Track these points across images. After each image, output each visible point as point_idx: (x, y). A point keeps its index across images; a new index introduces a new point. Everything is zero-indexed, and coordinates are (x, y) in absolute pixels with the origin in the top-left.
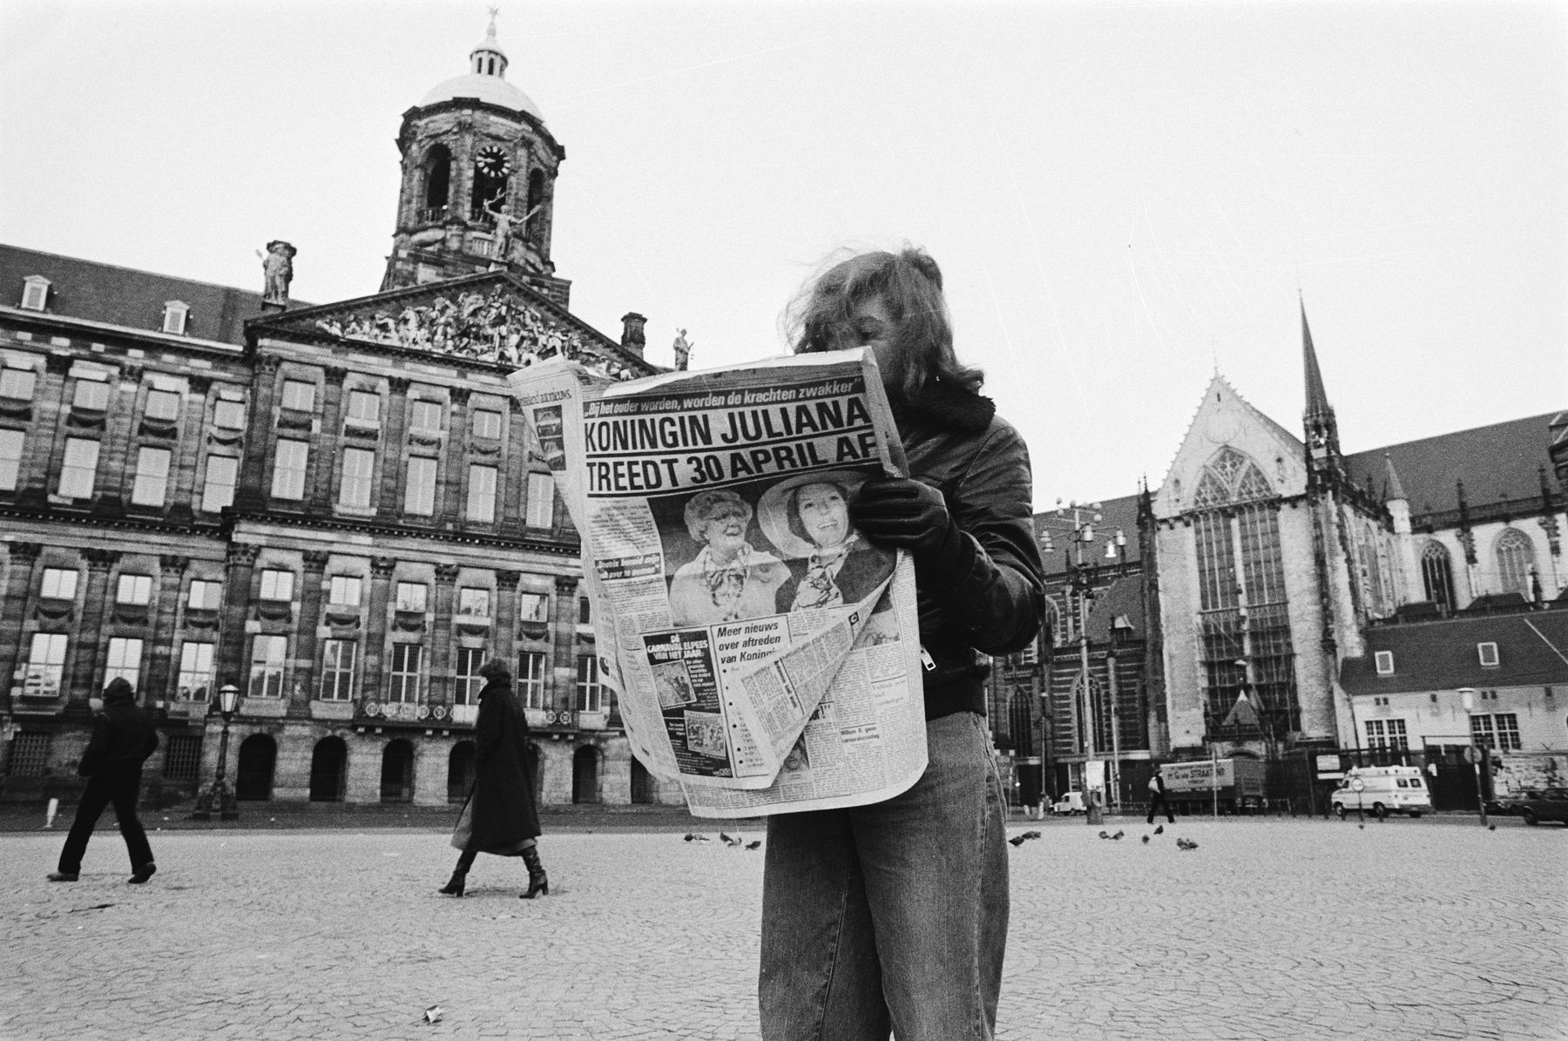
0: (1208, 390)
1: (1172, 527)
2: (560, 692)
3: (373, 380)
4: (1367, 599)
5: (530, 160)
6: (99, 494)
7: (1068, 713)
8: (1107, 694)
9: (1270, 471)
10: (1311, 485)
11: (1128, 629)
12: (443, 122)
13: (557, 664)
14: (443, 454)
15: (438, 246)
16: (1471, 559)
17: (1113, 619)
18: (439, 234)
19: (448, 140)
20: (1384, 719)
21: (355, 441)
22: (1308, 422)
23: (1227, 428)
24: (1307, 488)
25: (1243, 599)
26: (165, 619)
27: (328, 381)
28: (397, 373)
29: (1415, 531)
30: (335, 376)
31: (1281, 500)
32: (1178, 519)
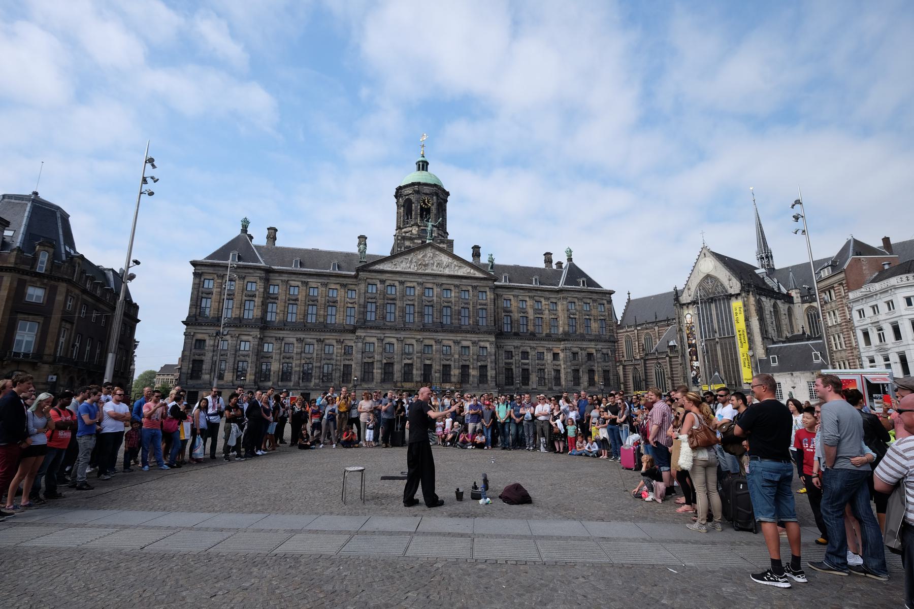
0: (701, 252)
1: (688, 307)
3: (393, 282)
4: (772, 332)
5: (437, 199)
7: (652, 378)
9: (726, 283)
10: (743, 289)
11: (675, 346)
14: (416, 304)
17: (668, 342)
18: (410, 229)
19: (412, 197)
21: (389, 302)
22: (759, 256)
23: (709, 266)
24: (741, 291)
25: (717, 335)
26: (339, 358)
28: (400, 279)
31: (731, 295)
32: (689, 304)
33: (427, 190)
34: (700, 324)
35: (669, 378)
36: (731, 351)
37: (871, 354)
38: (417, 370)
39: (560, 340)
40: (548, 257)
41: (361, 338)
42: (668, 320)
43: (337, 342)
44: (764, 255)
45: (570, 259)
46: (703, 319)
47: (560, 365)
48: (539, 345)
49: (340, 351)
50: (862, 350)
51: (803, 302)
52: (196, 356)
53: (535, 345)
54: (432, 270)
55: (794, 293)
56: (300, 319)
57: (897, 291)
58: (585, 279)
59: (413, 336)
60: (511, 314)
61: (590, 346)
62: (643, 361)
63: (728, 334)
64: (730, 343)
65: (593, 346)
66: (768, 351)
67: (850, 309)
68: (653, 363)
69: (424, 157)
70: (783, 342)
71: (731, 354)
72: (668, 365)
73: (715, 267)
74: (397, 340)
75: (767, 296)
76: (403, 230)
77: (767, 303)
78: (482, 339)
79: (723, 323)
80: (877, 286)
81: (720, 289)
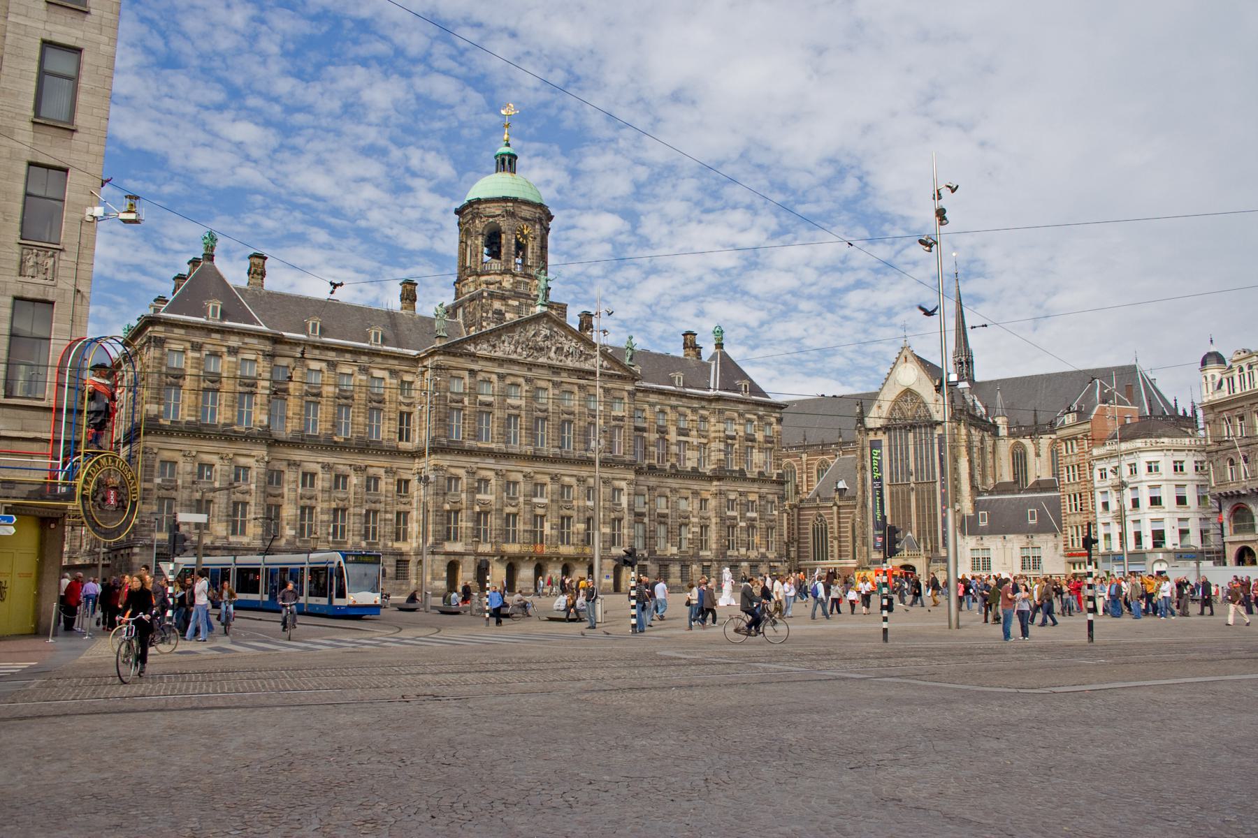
2: (581, 537)
3: (489, 375)
6: (355, 435)
8: (832, 528)
12: (495, 209)
13: (578, 522)
14: (523, 413)
15: (497, 285)
16: (1038, 455)
18: (498, 278)
20: (980, 547)
23: (909, 375)
25: (913, 479)
27: (470, 377)
29: (1011, 435)
30: (473, 373)
32: (879, 429)
33: (526, 212)
34: (891, 460)
35: (835, 538)
36: (929, 502)
37: (1107, 521)
38: (524, 523)
39: (710, 479)
40: (690, 340)
41: (442, 470)
42: (823, 445)
43: (386, 472)
44: (963, 359)
45: (719, 346)
46: (896, 454)
47: (709, 518)
48: (682, 486)
49: (390, 488)
50: (1098, 516)
51: (1011, 435)
52: (164, 491)
53: (678, 486)
54: (549, 358)
55: (1000, 421)
56: (326, 429)
57: (1141, 455)
58: (747, 383)
59: (519, 468)
60: (645, 434)
61: (752, 490)
62: (796, 510)
63: (928, 478)
64: (928, 491)
65: (756, 490)
66: (976, 506)
67: (1091, 468)
68: (811, 515)
69: (508, 145)
70: (991, 493)
71: (929, 507)
72: (836, 518)
73: (919, 379)
74: (497, 474)
75: (976, 427)
76: (483, 278)
77: (976, 435)
78: (618, 476)
79: (922, 463)
80: (1124, 446)
81: (922, 412)
